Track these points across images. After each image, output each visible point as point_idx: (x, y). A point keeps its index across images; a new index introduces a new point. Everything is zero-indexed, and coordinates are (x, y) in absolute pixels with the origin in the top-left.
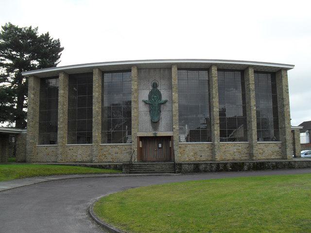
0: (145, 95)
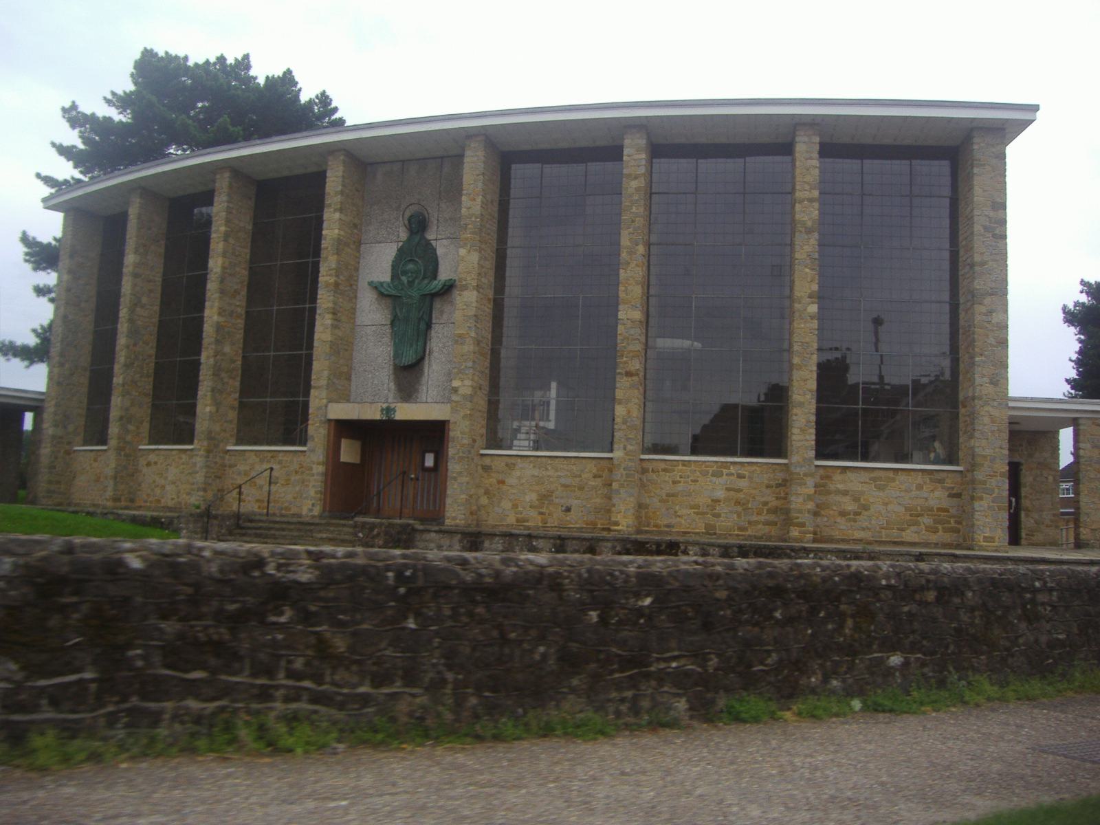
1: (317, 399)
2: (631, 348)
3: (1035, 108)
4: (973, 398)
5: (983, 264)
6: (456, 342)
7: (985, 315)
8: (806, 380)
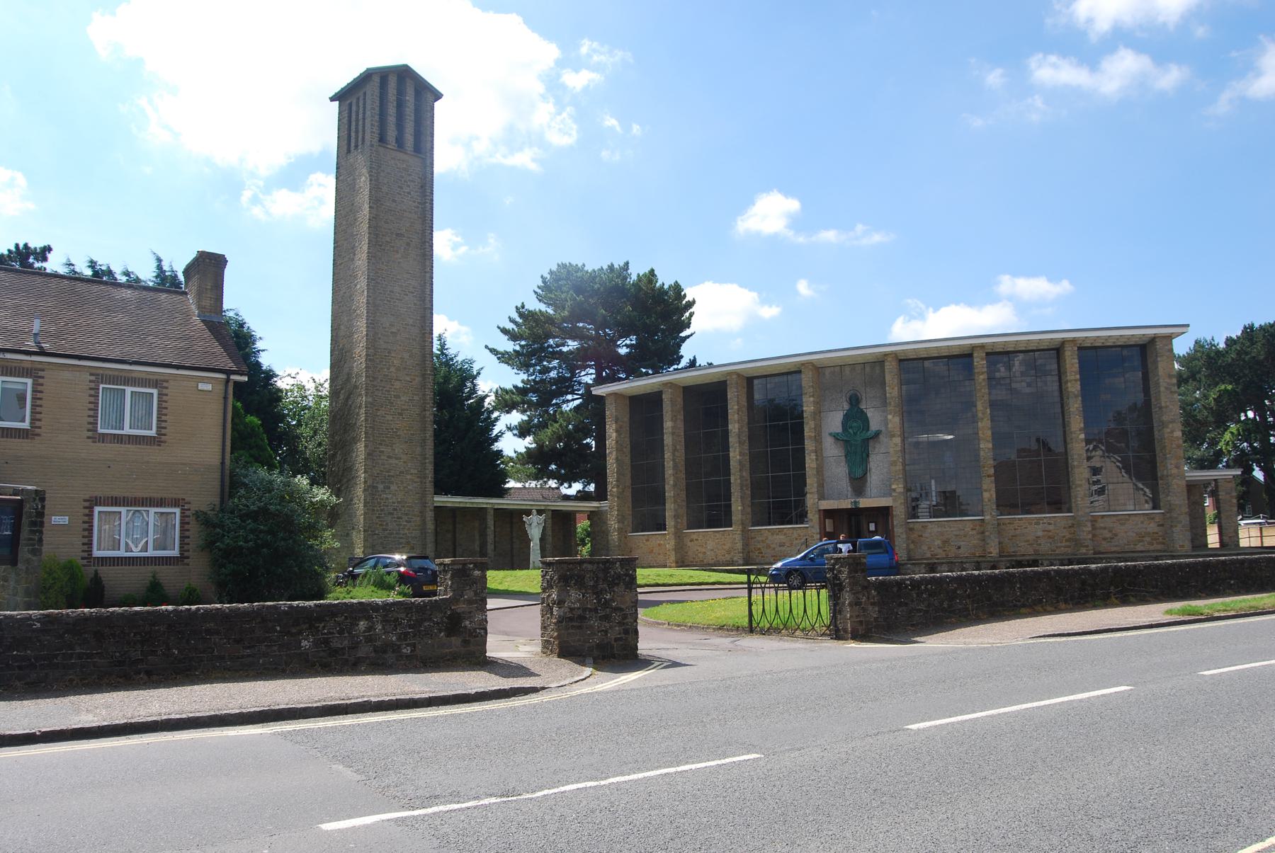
0: (835, 421)
1: (811, 500)
2: (988, 463)
4: (1167, 476)
5: (1167, 407)
6: (892, 465)
7: (1169, 433)
8: (1082, 473)
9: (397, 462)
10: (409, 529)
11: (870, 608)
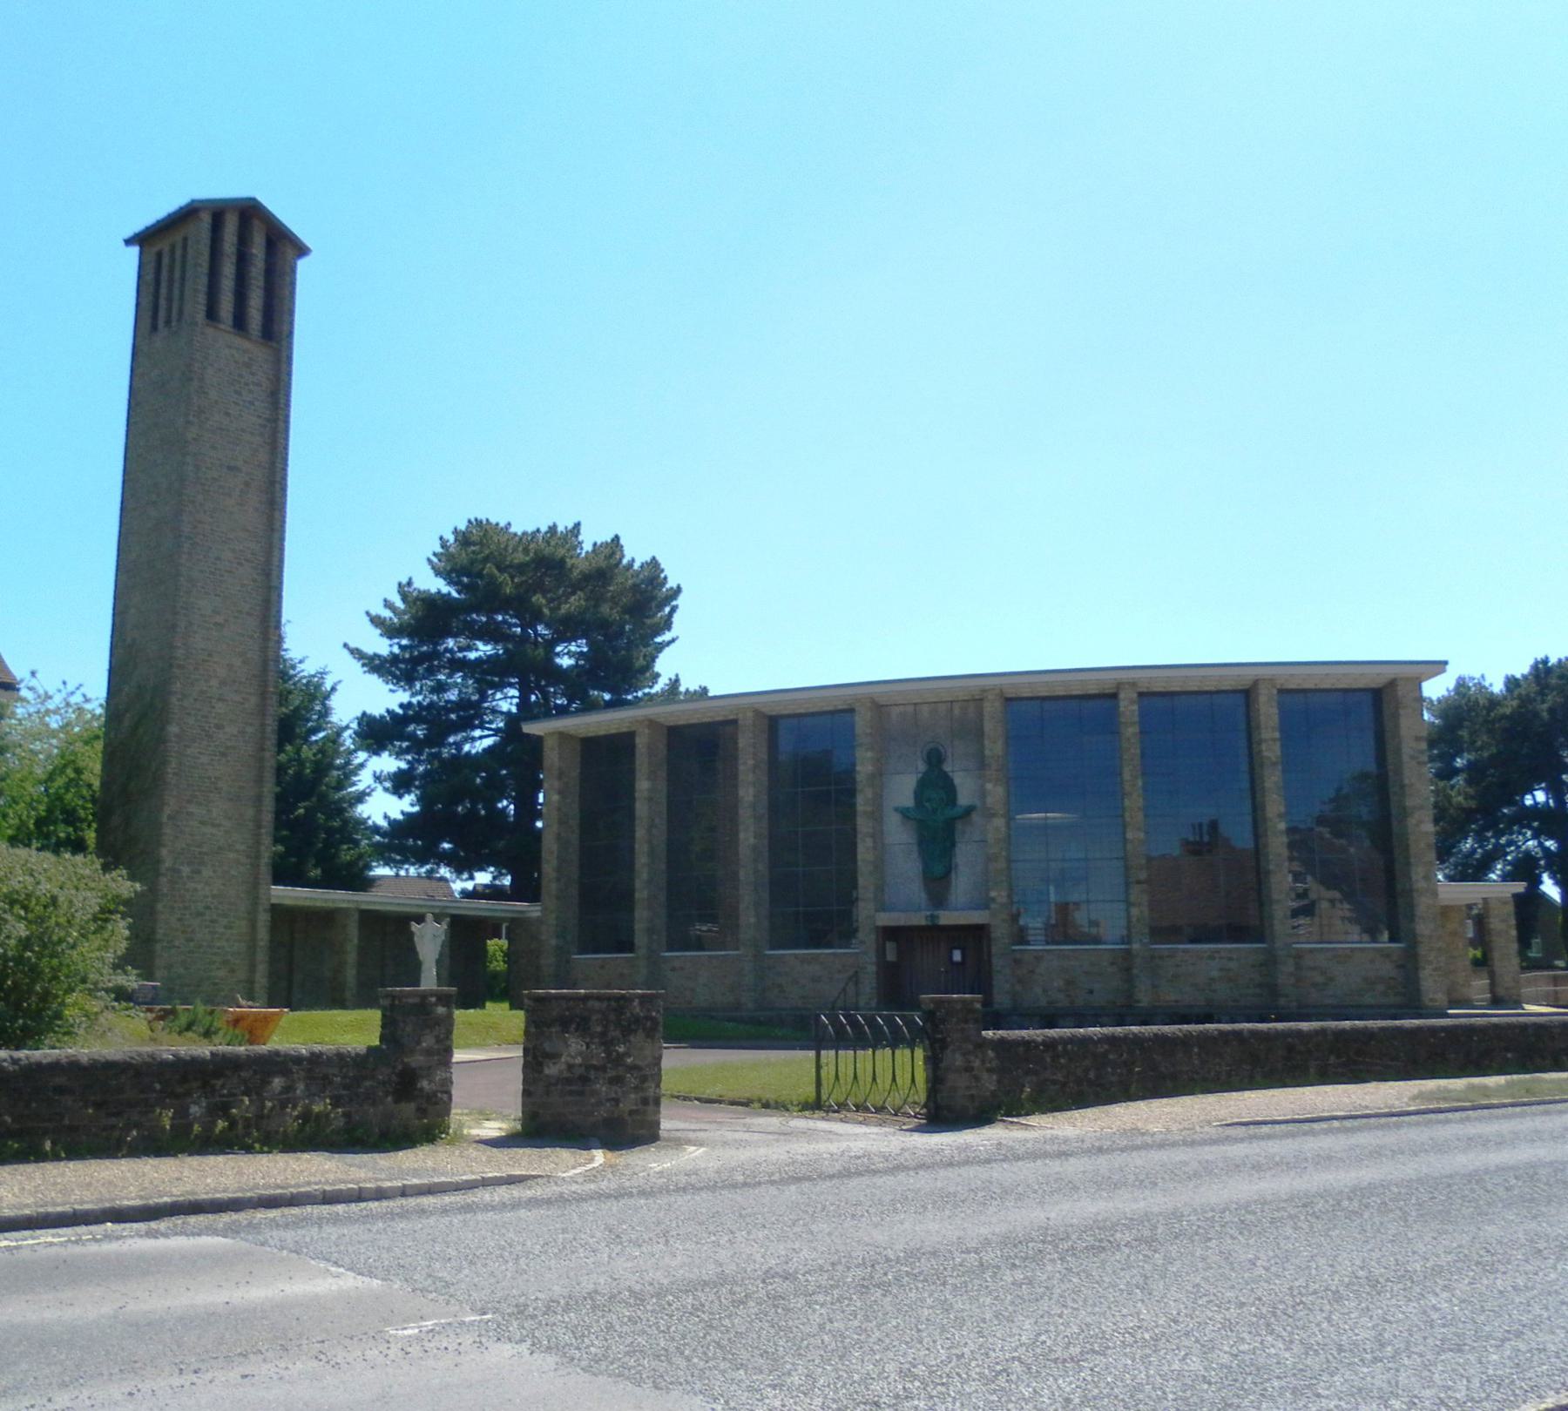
0: (903, 789)
3: (1446, 663)
9: (214, 831)
10: (227, 940)
11: (985, 1076)
